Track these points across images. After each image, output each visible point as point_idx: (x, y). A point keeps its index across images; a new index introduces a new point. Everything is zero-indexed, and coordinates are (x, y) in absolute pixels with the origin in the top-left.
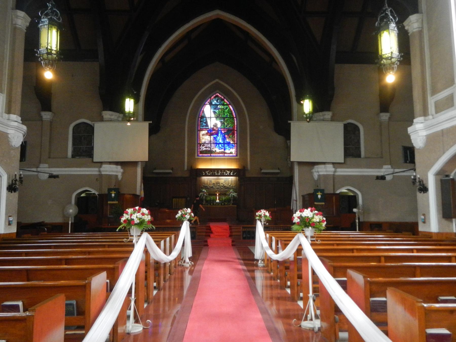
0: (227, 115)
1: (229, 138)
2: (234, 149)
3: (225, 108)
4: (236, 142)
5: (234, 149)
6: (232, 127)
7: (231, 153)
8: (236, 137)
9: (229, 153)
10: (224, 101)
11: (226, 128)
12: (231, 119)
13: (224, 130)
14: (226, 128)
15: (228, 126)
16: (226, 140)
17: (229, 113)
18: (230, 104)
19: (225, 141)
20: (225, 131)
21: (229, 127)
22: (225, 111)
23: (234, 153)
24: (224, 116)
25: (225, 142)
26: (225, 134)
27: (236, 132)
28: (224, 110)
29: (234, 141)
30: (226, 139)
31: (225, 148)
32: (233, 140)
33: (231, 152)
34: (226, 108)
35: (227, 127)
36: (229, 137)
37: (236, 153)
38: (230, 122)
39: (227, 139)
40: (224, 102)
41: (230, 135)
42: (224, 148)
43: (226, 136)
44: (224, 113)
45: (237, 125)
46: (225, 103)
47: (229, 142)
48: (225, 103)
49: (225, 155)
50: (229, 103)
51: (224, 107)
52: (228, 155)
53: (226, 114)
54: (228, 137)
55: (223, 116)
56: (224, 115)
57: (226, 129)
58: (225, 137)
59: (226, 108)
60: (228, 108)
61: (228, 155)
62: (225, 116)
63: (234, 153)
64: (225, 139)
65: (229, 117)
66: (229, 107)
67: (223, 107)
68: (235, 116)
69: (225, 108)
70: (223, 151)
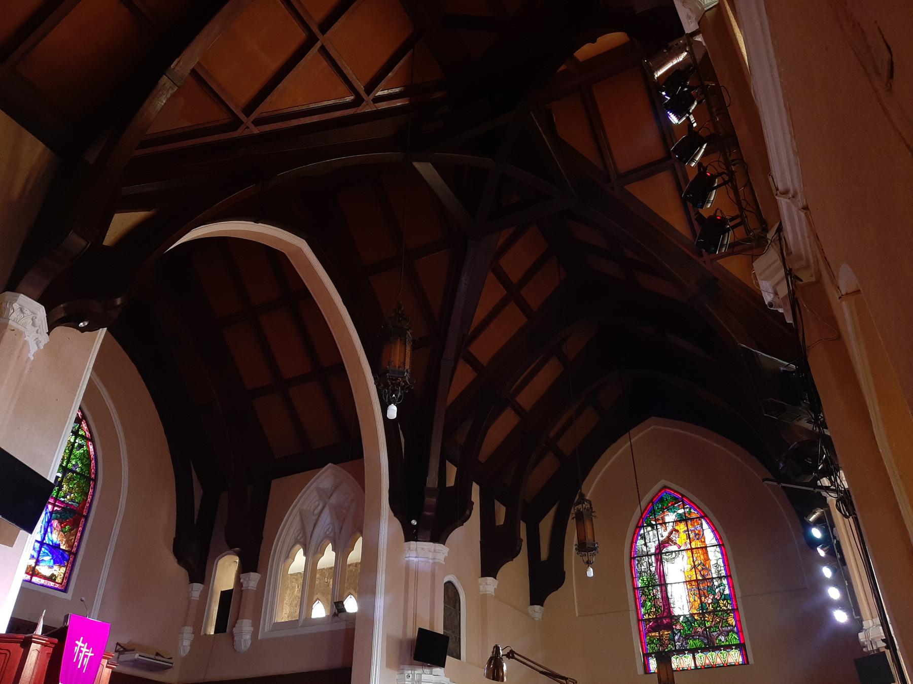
1: (62, 531)
2: (63, 570)
3: (76, 444)
4: (74, 550)
5: (63, 570)
6: (77, 503)
7: (52, 578)
8: (79, 534)
9: (45, 578)
10: (80, 426)
11: (62, 499)
12: (82, 481)
13: (54, 505)
14: (62, 499)
15: (68, 497)
16: (50, 534)
17: (82, 463)
18: (91, 440)
19: (46, 538)
20: (56, 508)
21: (72, 500)
22: (74, 450)
23: (59, 580)
24: (68, 463)
25: (46, 541)
26: (54, 515)
27: (83, 520)
29: (72, 547)
30: (51, 533)
31: (41, 558)
32: (67, 542)
33: (53, 575)
34: (81, 446)
35: (64, 497)
36: (62, 527)
39: (55, 532)
40: (79, 427)
41: (66, 525)
42: (39, 556)
43: (55, 523)
45: (92, 500)
46: (81, 433)
47: (55, 544)
48: (81, 433)
49: (35, 579)
50: (92, 435)
51: (75, 440)
52: (42, 581)
53: (74, 463)
57: (63, 502)
58: (52, 525)
59: (81, 446)
60: (85, 448)
61: (42, 581)
62: (70, 466)
63: (59, 580)
64: (49, 530)
66: (88, 447)
68: (93, 476)
69: (76, 444)
70: (33, 565)
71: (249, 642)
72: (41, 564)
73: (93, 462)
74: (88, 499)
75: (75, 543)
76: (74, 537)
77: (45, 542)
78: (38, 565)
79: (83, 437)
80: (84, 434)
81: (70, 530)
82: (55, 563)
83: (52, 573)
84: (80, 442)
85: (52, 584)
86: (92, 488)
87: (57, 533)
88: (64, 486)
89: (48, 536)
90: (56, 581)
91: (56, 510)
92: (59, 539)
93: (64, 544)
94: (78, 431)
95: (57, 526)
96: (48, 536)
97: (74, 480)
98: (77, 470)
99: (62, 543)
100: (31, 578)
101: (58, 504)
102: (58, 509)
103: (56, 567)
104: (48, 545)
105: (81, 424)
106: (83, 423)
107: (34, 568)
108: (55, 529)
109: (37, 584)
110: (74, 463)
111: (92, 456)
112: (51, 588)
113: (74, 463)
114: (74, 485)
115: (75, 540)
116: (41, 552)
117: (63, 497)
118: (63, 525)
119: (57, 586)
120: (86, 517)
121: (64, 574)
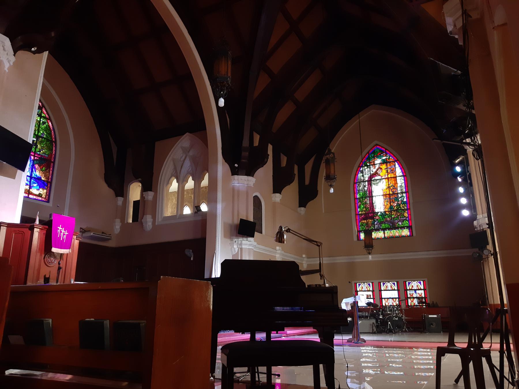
0: (43, 134)
1: (41, 170)
2: (45, 191)
3: (41, 122)
5: (45, 191)
6: (47, 155)
7: (40, 195)
8: (51, 172)
10: (41, 111)
11: (39, 153)
13: (34, 156)
14: (39, 153)
16: (34, 172)
17: (46, 133)
18: (49, 119)
19: (33, 174)
20: (36, 158)
21: (44, 153)
23: (44, 196)
25: (33, 176)
26: (35, 162)
27: (52, 164)
28: (40, 124)
30: (35, 171)
33: (40, 194)
34: (44, 123)
35: (40, 152)
36: (41, 168)
37: (47, 197)
38: (46, 146)
40: (41, 112)
41: (42, 167)
43: (37, 166)
44: (39, 128)
46: (43, 115)
48: (43, 115)
49: (31, 196)
51: (40, 119)
52: (35, 197)
54: (39, 169)
55: (36, 133)
56: (39, 132)
57: (39, 155)
59: (44, 123)
60: (47, 124)
61: (35, 197)
62: (40, 134)
64: (34, 170)
65: (45, 139)
67: (39, 120)
68: (54, 140)
69: (41, 122)
70: (28, 189)
71: (151, 227)
72: (32, 188)
73: (53, 132)
74: (53, 153)
75: (50, 177)
76: (48, 173)
77: (32, 176)
78: (31, 189)
79: (45, 118)
80: (45, 116)
81: (46, 170)
82: (40, 187)
83: (39, 192)
84: (43, 121)
85: (40, 198)
86: (54, 147)
87: (39, 172)
88: (39, 145)
89: (34, 173)
90: (42, 197)
91: (36, 159)
92: (40, 175)
93: (44, 177)
94: (41, 114)
95: (38, 168)
96: (34, 173)
97: (44, 142)
98: (44, 136)
99: (42, 177)
100: (28, 196)
101: (37, 156)
102: (37, 158)
103: (41, 190)
104: (35, 178)
105: (42, 110)
106: (43, 109)
107: (29, 190)
108: (37, 169)
109: (32, 199)
110: (41, 132)
111: (51, 128)
112: (40, 200)
113: (41, 132)
114: (44, 145)
115: (49, 175)
116: (32, 182)
117: (39, 152)
118: (41, 167)
119: (43, 199)
120: (54, 163)
121: (46, 193)
